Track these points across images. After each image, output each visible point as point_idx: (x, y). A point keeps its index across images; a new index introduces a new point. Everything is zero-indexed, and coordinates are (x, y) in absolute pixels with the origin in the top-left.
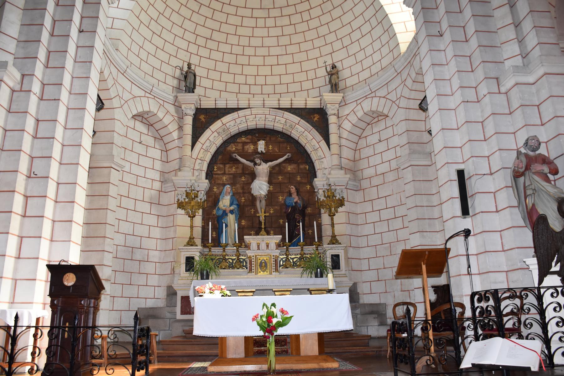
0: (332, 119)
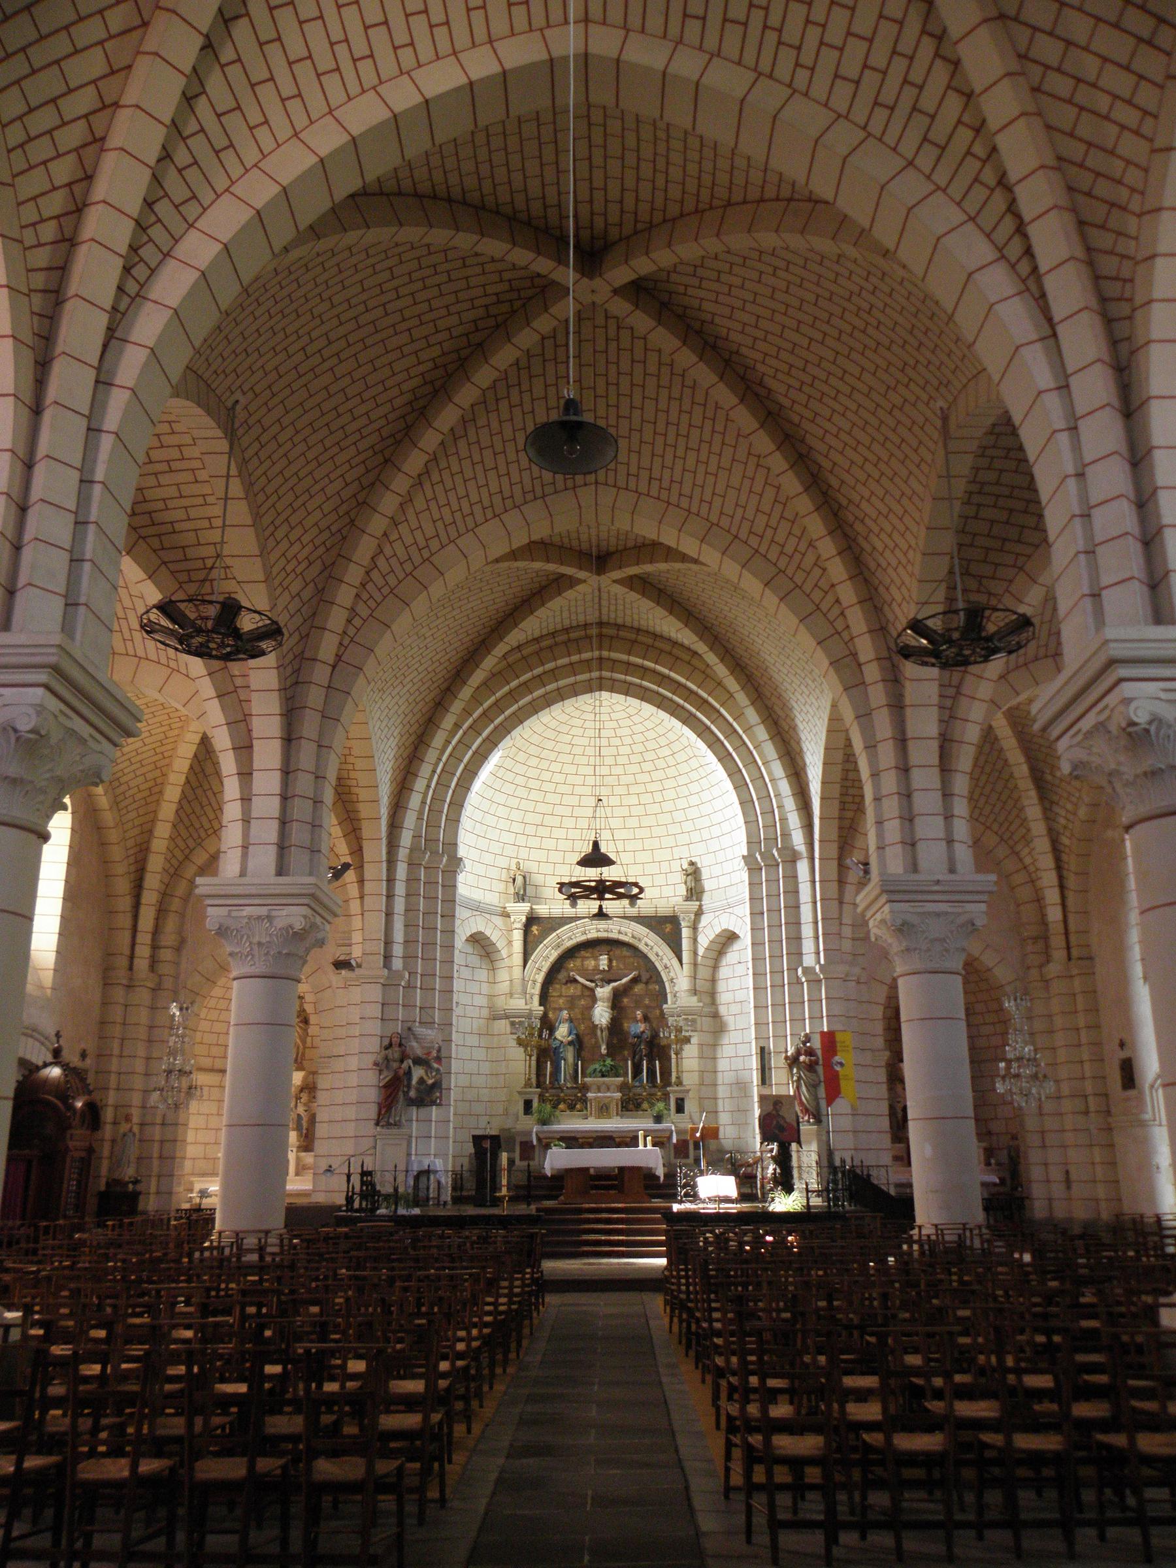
0: (685, 933)
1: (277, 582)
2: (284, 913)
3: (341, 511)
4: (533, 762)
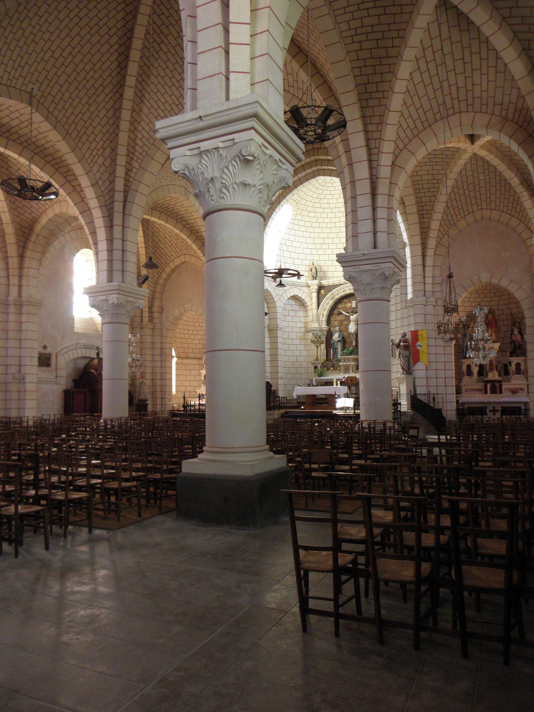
1: (89, 161)
2: (111, 297)
3: (111, 122)
4: (312, 214)
